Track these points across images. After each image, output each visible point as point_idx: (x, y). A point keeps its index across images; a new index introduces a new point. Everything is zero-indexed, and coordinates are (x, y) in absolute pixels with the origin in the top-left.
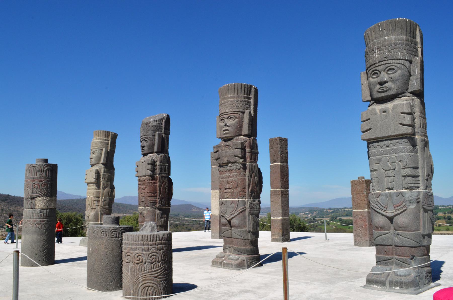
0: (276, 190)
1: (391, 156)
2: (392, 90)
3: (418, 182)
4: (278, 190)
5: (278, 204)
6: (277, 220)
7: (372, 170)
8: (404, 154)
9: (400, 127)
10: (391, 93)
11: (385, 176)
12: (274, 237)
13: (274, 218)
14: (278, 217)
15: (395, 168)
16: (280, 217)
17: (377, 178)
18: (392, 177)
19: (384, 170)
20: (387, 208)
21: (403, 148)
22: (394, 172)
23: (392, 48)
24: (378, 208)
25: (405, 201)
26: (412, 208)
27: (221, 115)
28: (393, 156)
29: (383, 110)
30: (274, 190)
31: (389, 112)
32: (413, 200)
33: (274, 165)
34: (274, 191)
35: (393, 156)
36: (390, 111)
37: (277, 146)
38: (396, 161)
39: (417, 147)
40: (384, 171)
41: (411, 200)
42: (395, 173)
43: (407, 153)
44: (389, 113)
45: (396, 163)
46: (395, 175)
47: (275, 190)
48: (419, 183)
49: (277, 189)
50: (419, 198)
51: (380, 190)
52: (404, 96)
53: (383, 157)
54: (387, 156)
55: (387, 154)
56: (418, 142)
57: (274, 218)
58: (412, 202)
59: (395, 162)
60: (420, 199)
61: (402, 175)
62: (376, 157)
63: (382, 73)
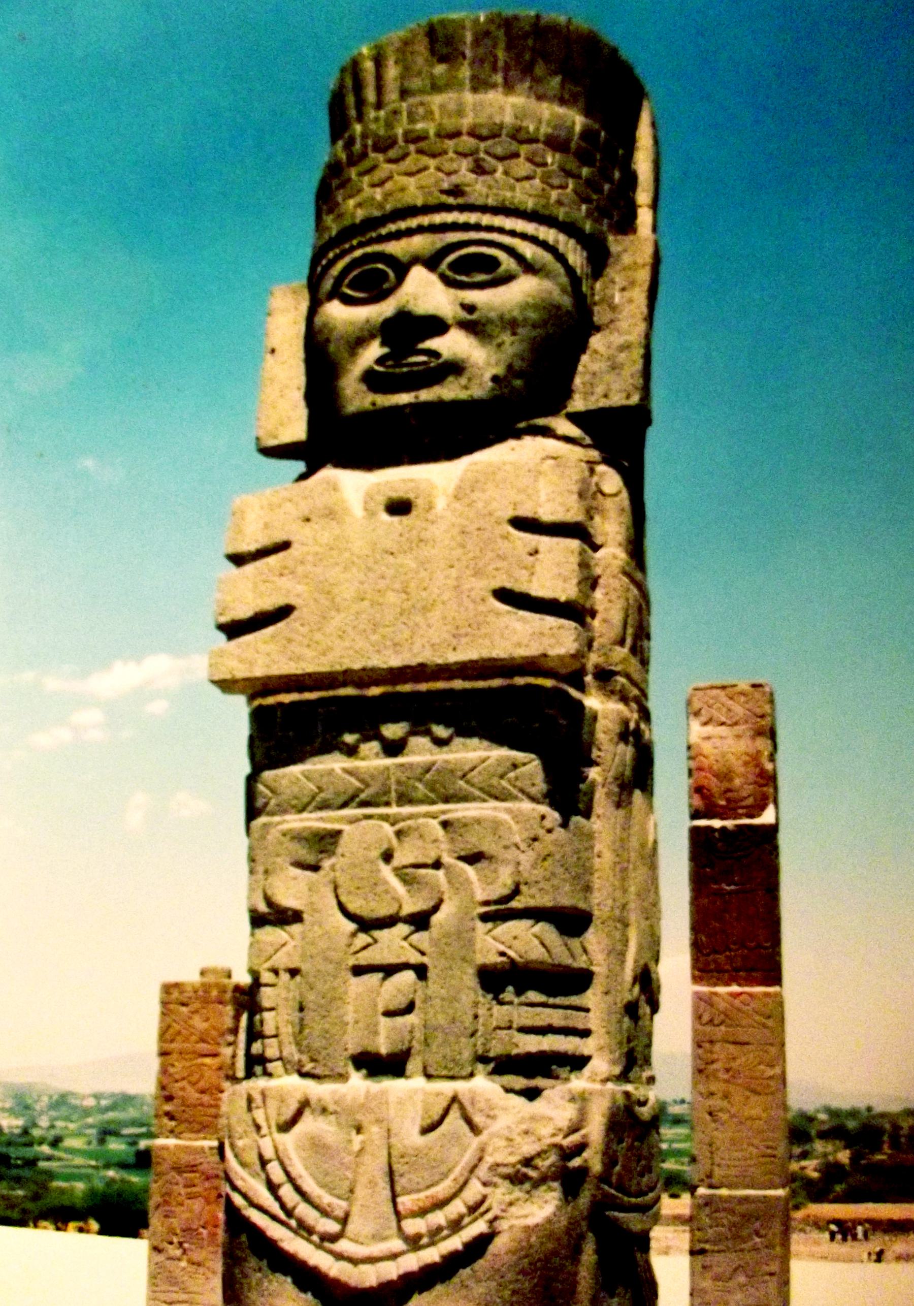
1: (411, 817)
2: (470, 379)
3: (577, 1020)
7: (263, 907)
8: (509, 811)
9: (498, 614)
10: (463, 395)
11: (352, 961)
15: (436, 909)
17: (294, 972)
18: (409, 976)
19: (350, 916)
20: (344, 1221)
21: (499, 762)
22: (420, 938)
23: (499, 150)
24: (282, 1216)
25: (483, 1171)
26: (531, 1221)
28: (427, 815)
29: (395, 495)
31: (430, 507)
32: (538, 1162)
35: (427, 815)
36: (441, 504)
38: (447, 859)
39: (594, 773)
40: (352, 926)
41: (528, 1162)
42: (425, 946)
43: (527, 806)
44: (430, 517)
45: (441, 873)
46: (425, 960)
48: (585, 1033)
50: (580, 1148)
51: (308, 1067)
52: (547, 432)
53: (353, 821)
54: (385, 818)
55: (387, 804)
56: (600, 736)
58: (533, 1173)
59: (437, 865)
60: (585, 1154)
61: (480, 959)
62: (305, 815)
63: (418, 273)
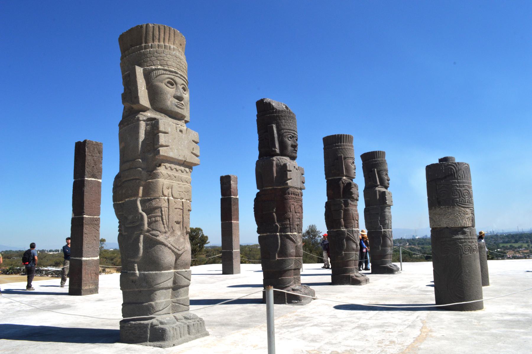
0: (93, 218)
4: (96, 218)
5: (95, 239)
6: (93, 260)
12: (88, 288)
13: (88, 259)
14: (95, 257)
16: (97, 257)
27: (352, 158)
30: (90, 217)
33: (91, 180)
34: (90, 218)
37: (98, 154)
47: (92, 217)
49: (95, 217)
57: (88, 259)
